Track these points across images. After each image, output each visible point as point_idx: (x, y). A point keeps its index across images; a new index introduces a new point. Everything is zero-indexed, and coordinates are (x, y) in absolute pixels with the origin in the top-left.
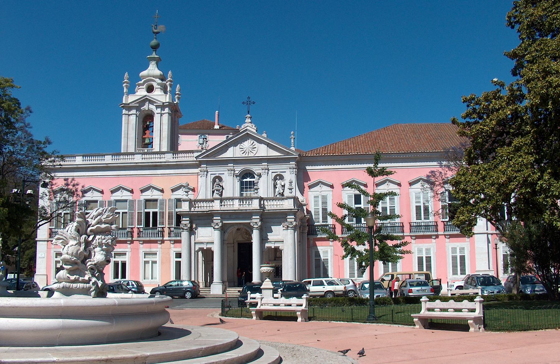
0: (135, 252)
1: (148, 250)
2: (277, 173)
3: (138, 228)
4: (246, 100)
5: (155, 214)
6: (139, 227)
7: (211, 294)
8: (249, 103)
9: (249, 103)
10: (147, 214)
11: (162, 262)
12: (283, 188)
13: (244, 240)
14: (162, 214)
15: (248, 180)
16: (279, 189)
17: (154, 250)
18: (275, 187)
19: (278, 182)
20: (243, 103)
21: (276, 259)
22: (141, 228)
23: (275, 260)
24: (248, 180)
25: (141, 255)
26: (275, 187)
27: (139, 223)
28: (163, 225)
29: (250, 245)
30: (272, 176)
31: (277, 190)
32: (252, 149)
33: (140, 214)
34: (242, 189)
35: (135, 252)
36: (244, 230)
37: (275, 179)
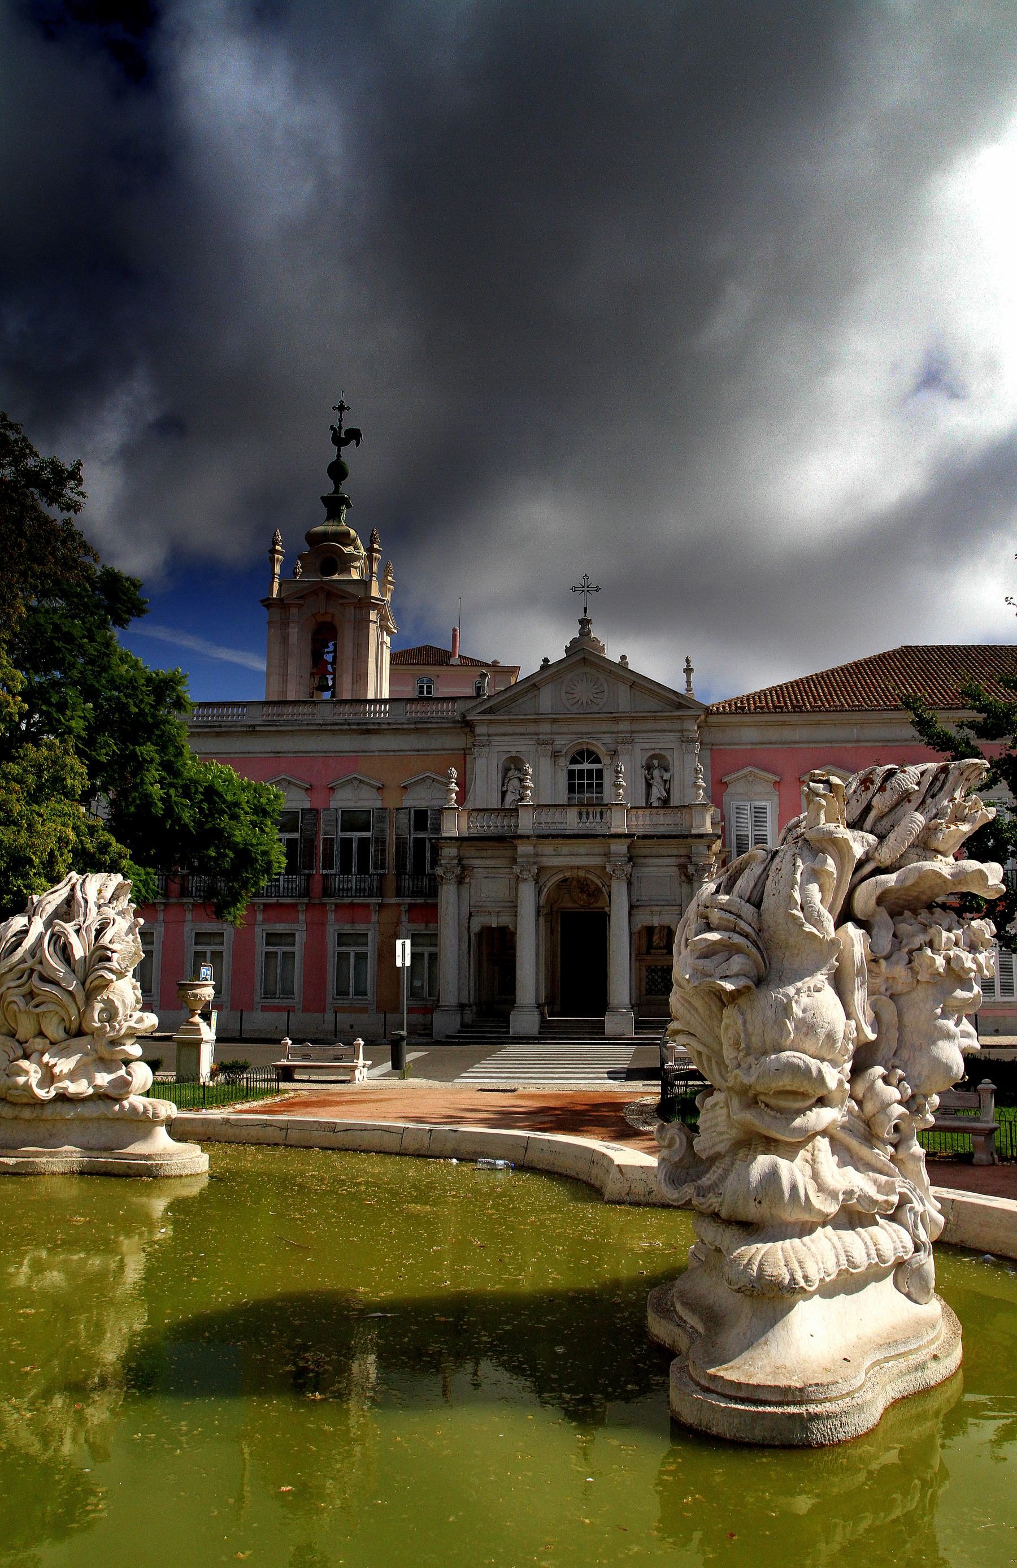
0: (317, 929)
1: (347, 928)
2: (653, 752)
3: (325, 877)
4: (578, 581)
5: (364, 843)
6: (325, 872)
7: (511, 1034)
8: (586, 589)
9: (586, 589)
10: (346, 843)
11: (379, 955)
12: (667, 787)
13: (576, 905)
14: (381, 841)
15: (586, 766)
16: (657, 791)
17: (360, 928)
18: (649, 786)
19: (656, 773)
20: (574, 589)
21: (653, 951)
22: (331, 875)
23: (648, 953)
24: (586, 766)
25: (331, 939)
26: (649, 786)
27: (328, 864)
28: (383, 867)
29: (601, 921)
30: (640, 758)
31: (655, 790)
32: (596, 696)
33: (329, 843)
34: (571, 789)
35: (317, 929)
36: (575, 883)
37: (649, 768)
